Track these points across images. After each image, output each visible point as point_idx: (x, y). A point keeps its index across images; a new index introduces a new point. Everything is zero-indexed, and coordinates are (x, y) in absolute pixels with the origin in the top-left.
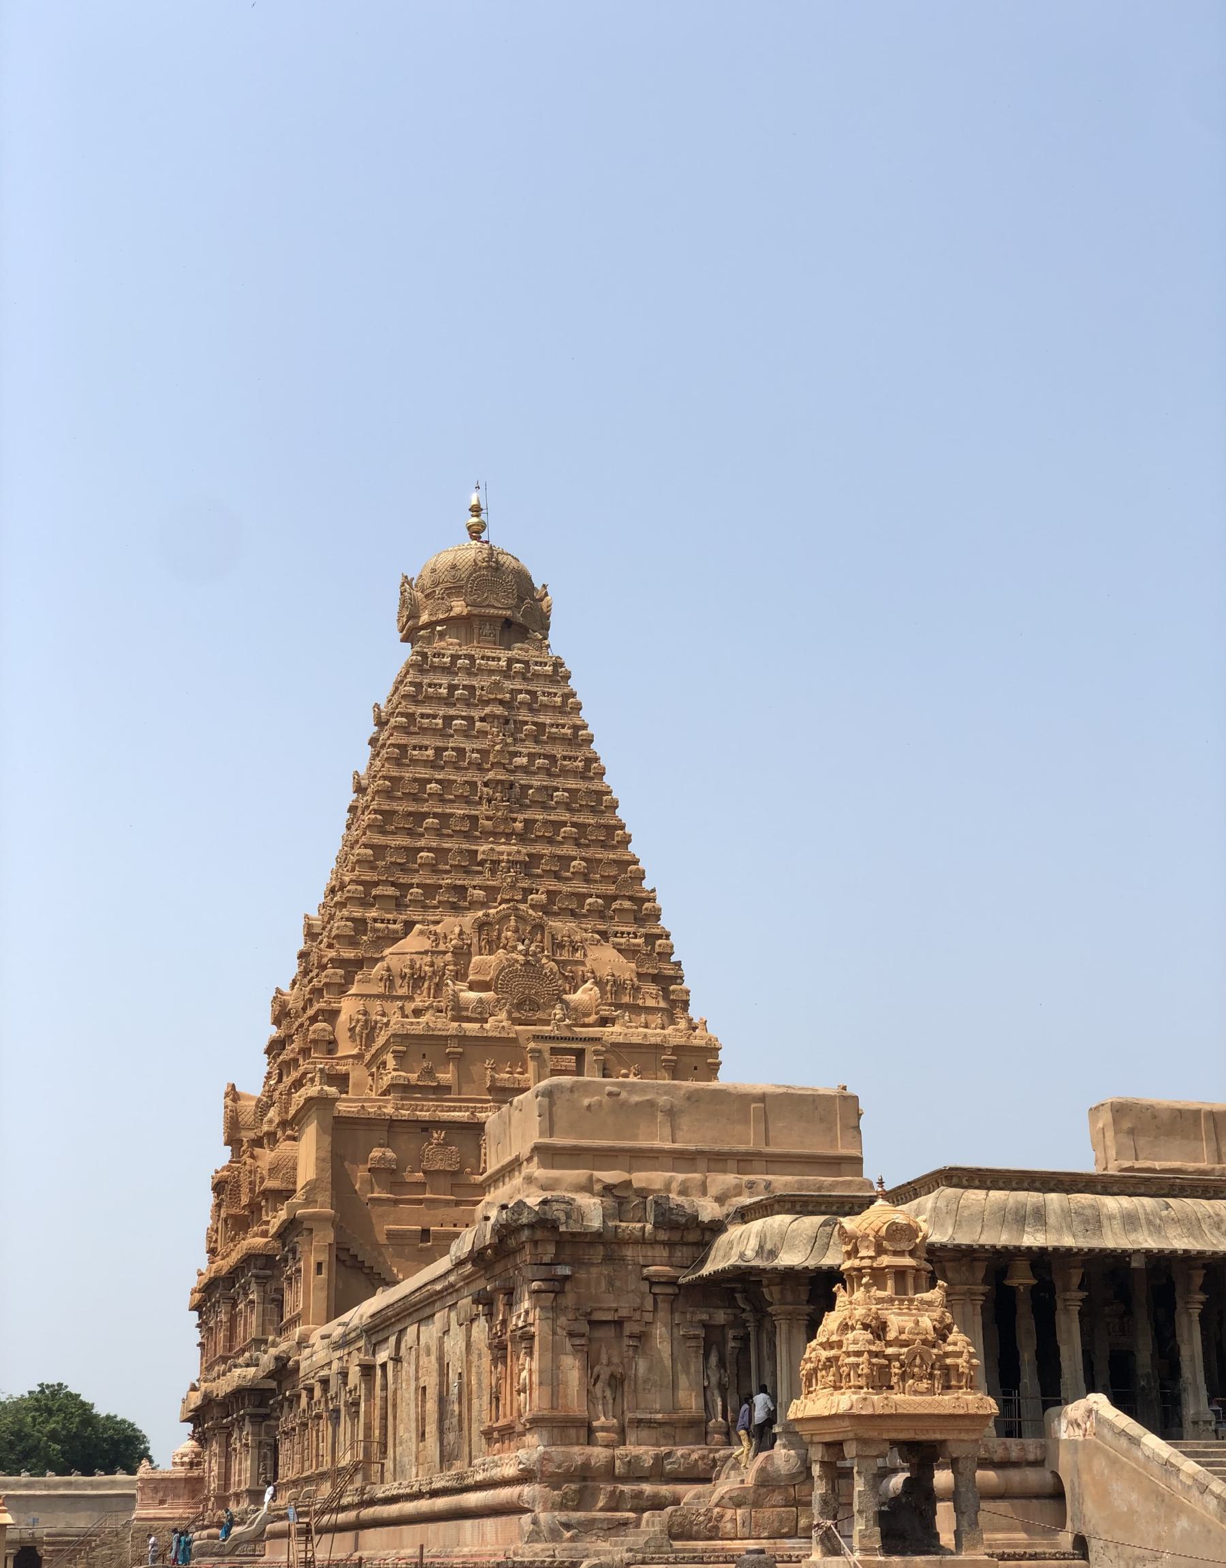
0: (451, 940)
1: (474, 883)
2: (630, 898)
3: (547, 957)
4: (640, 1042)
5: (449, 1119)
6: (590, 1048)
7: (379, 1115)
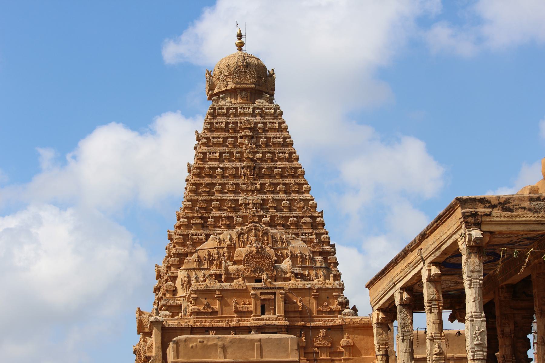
0: (226, 242)
1: (238, 214)
2: (309, 217)
3: (270, 247)
4: (302, 287)
5: (217, 326)
6: (278, 291)
7: (187, 326)
